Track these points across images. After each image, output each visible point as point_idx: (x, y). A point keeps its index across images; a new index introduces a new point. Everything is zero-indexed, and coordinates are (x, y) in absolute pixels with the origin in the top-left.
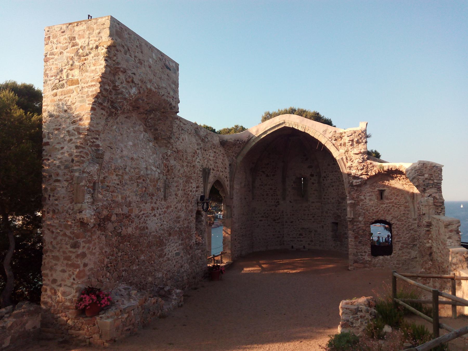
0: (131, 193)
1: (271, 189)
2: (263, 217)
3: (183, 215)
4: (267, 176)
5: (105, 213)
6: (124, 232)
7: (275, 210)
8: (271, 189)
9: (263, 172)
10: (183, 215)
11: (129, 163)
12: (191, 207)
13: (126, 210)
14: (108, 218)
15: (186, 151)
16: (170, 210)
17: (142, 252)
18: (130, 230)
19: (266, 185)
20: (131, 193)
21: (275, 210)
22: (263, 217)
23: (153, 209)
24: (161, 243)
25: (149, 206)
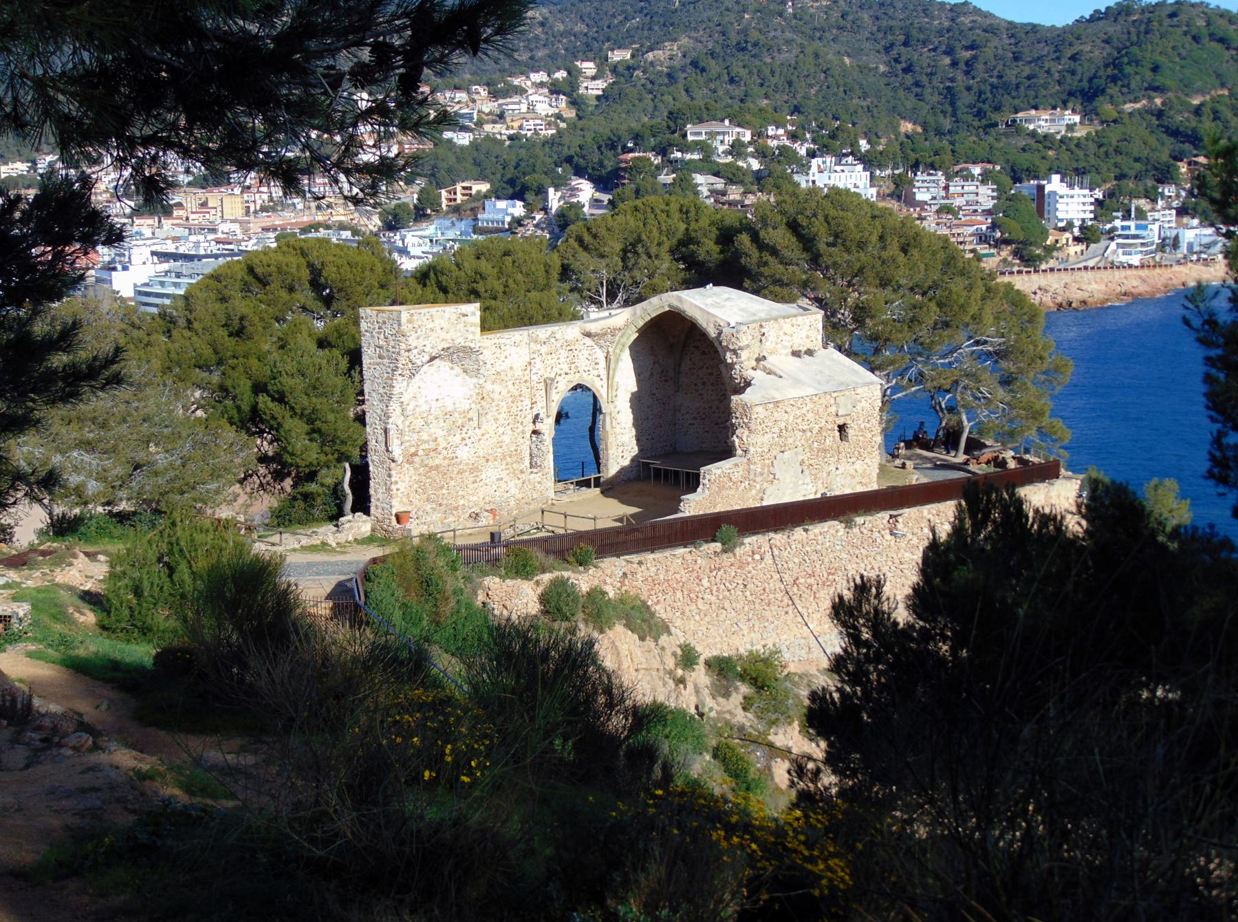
0: (437, 430)
1: (711, 374)
2: (695, 418)
3: (507, 439)
4: (704, 353)
5: (413, 450)
6: (431, 463)
7: (718, 408)
8: (711, 374)
9: (697, 347)
10: (507, 439)
11: (434, 404)
12: (521, 428)
13: (433, 445)
14: (415, 454)
15: (511, 368)
16: (487, 436)
17: (452, 478)
18: (437, 461)
19: (702, 368)
20: (437, 430)
21: (718, 408)
22: (695, 418)
23: (463, 439)
24: (475, 470)
25: (458, 437)
